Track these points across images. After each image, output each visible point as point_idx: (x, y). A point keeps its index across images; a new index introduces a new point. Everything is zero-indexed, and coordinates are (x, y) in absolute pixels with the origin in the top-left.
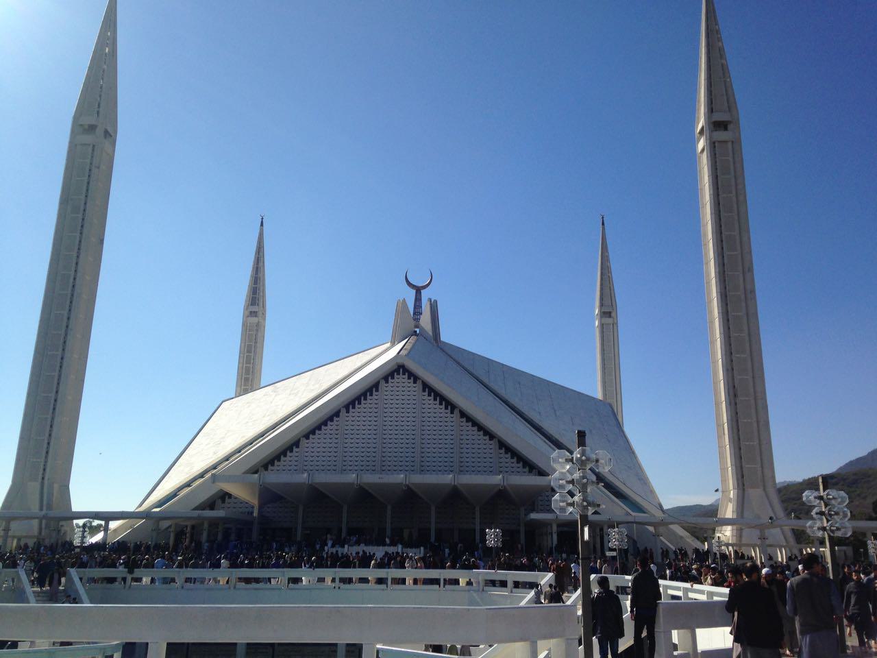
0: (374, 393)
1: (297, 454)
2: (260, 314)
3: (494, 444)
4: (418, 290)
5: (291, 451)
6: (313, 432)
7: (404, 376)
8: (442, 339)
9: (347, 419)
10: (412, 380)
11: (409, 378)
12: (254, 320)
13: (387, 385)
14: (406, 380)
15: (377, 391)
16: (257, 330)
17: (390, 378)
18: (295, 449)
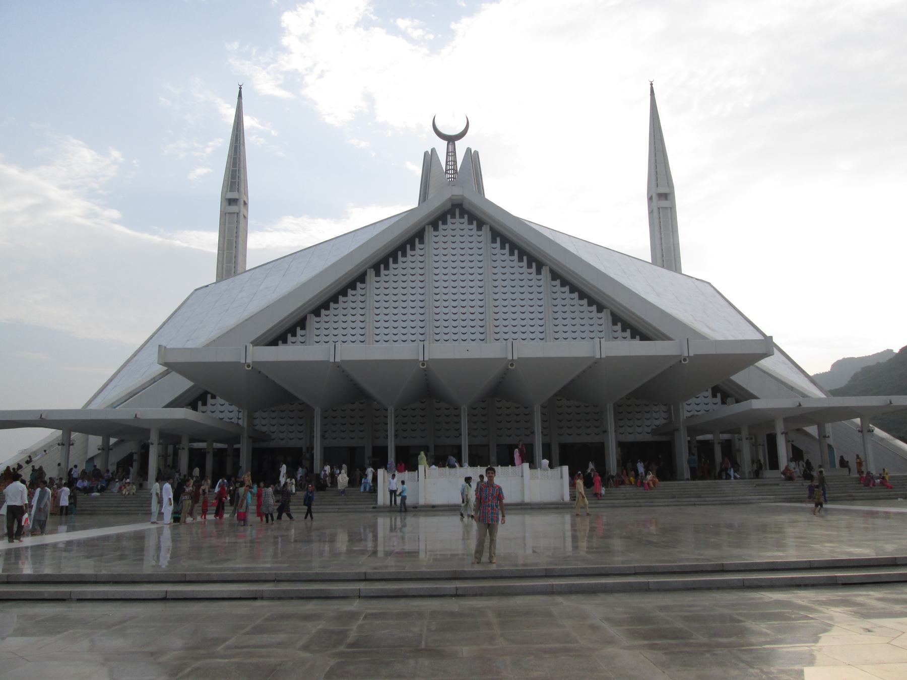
0: (418, 246)
1: (302, 339)
3: (605, 315)
4: (451, 140)
5: (294, 335)
6: (325, 306)
7: (462, 220)
9: (378, 285)
11: (470, 223)
12: (233, 208)
13: (436, 233)
14: (466, 226)
15: (422, 242)
16: (238, 222)
17: (440, 223)
18: (299, 332)
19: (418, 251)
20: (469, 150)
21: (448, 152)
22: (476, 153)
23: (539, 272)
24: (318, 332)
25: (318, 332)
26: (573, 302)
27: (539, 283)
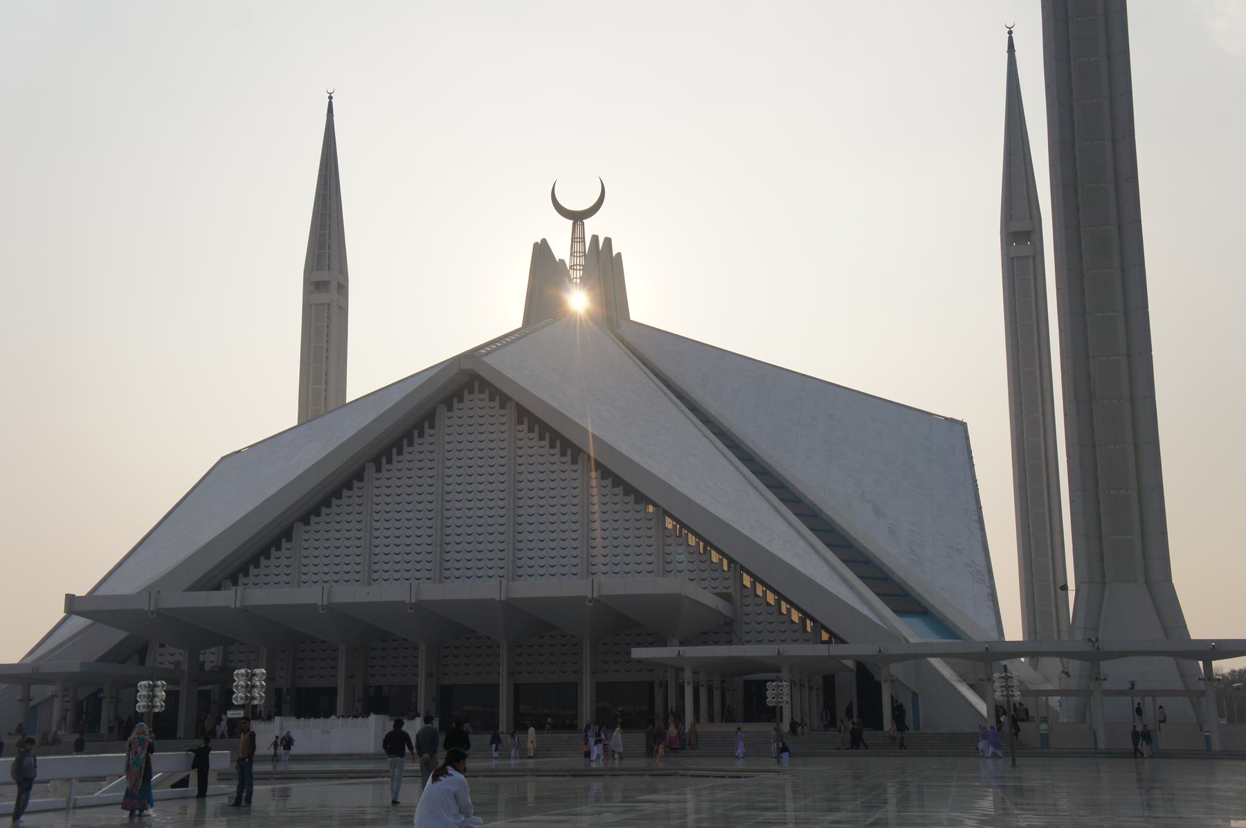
0: (427, 431)
1: (288, 554)
2: (334, 286)
4: (577, 218)
5: (279, 548)
6: (316, 511)
7: (482, 396)
8: (635, 315)
9: (378, 483)
10: (496, 403)
11: (491, 399)
13: (450, 414)
15: (432, 426)
17: (455, 400)
18: (285, 544)
19: (427, 439)
20: (595, 239)
21: (573, 239)
22: (608, 241)
23: (574, 462)
24: (306, 544)
25: (306, 544)
26: (616, 499)
27: (574, 475)
